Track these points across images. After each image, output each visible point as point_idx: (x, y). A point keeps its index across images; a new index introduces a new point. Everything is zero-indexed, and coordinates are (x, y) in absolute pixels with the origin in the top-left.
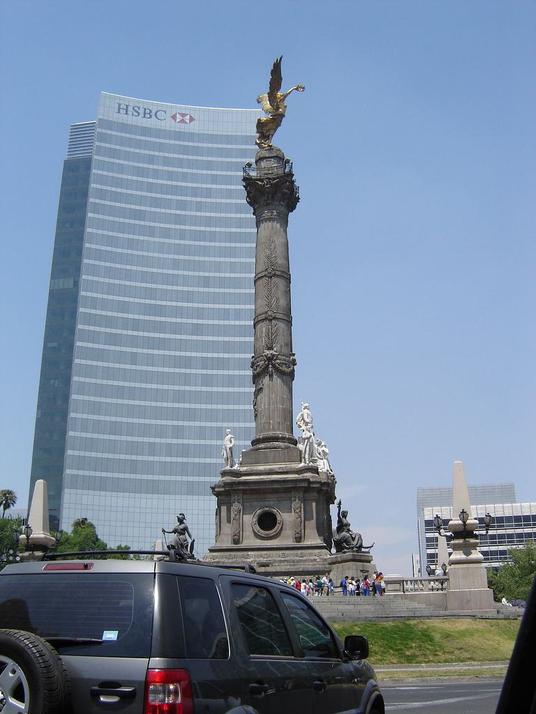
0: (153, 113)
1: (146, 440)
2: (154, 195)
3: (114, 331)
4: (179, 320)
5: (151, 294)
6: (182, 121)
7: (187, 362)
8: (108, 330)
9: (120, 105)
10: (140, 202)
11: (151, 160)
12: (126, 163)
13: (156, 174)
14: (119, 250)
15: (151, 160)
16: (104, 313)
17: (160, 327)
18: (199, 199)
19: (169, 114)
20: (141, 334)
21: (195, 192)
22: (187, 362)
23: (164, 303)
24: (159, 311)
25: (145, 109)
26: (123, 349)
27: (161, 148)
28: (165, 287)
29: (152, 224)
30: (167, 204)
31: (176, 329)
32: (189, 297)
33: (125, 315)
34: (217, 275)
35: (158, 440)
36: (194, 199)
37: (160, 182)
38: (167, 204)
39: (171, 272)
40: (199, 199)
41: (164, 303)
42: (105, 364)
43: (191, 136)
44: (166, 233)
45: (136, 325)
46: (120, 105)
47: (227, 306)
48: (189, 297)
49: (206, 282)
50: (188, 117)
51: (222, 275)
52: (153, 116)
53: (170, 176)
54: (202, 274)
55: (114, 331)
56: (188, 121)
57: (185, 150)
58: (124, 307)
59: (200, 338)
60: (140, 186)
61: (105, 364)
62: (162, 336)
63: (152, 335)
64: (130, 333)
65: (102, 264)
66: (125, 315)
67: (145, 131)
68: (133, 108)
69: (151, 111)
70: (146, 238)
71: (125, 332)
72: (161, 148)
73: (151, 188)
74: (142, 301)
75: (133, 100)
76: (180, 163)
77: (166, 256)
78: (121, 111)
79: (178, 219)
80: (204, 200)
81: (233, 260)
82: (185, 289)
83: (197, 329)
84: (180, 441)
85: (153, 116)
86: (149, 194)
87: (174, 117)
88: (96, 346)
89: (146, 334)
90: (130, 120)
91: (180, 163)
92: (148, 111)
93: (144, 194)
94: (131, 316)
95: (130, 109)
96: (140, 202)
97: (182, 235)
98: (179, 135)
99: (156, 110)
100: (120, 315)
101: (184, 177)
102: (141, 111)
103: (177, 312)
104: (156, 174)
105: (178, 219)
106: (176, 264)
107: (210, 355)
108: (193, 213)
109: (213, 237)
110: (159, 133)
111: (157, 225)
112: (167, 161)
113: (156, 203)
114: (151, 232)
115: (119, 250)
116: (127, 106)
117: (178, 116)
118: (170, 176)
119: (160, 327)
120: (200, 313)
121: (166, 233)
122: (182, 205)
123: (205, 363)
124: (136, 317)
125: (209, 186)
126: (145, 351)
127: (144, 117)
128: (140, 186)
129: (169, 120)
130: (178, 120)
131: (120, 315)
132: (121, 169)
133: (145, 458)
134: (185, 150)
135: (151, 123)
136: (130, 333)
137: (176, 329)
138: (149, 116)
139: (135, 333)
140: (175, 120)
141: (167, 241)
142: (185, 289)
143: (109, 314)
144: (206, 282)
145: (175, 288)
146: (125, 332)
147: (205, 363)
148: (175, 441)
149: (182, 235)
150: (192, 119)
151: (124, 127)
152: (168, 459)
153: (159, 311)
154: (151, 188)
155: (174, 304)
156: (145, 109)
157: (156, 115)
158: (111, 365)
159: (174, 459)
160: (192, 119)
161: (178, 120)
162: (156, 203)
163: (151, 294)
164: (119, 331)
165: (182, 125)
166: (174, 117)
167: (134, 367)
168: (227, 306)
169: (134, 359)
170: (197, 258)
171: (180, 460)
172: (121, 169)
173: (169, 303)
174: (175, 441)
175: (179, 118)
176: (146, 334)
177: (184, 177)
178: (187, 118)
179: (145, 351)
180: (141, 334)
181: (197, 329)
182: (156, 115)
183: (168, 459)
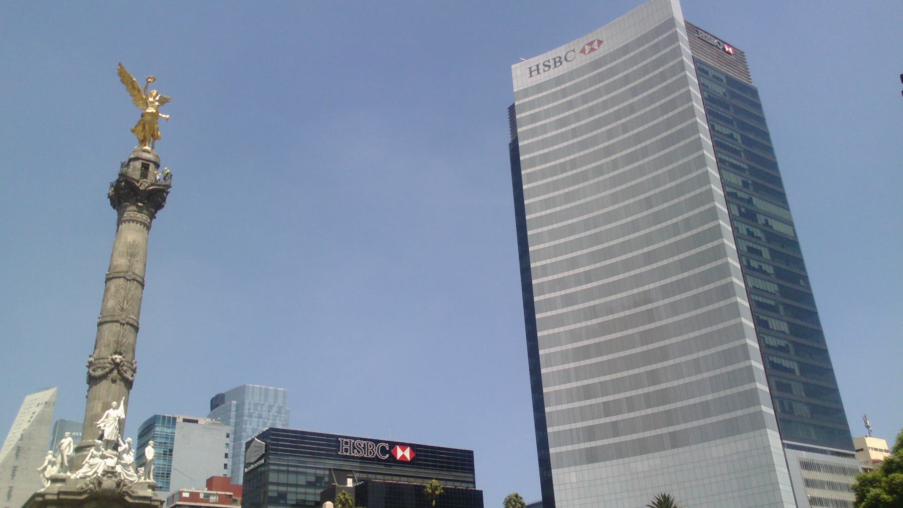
0: (563, 59)
3: (568, 291)
6: (592, 50)
19: (578, 51)
46: (530, 68)
50: (596, 43)
52: (564, 62)
55: (568, 291)
56: (596, 47)
68: (544, 65)
69: (560, 58)
75: (539, 59)
78: (533, 73)
85: (564, 62)
88: (554, 313)
92: (557, 60)
95: (541, 67)
99: (565, 53)
102: (552, 63)
116: (538, 66)
127: (555, 67)
133: (626, 416)
138: (559, 64)
140: (585, 53)
148: (652, 389)
150: (600, 42)
157: (566, 59)
165: (593, 54)
166: (583, 51)
171: (661, 408)
174: (652, 389)
182: (566, 59)
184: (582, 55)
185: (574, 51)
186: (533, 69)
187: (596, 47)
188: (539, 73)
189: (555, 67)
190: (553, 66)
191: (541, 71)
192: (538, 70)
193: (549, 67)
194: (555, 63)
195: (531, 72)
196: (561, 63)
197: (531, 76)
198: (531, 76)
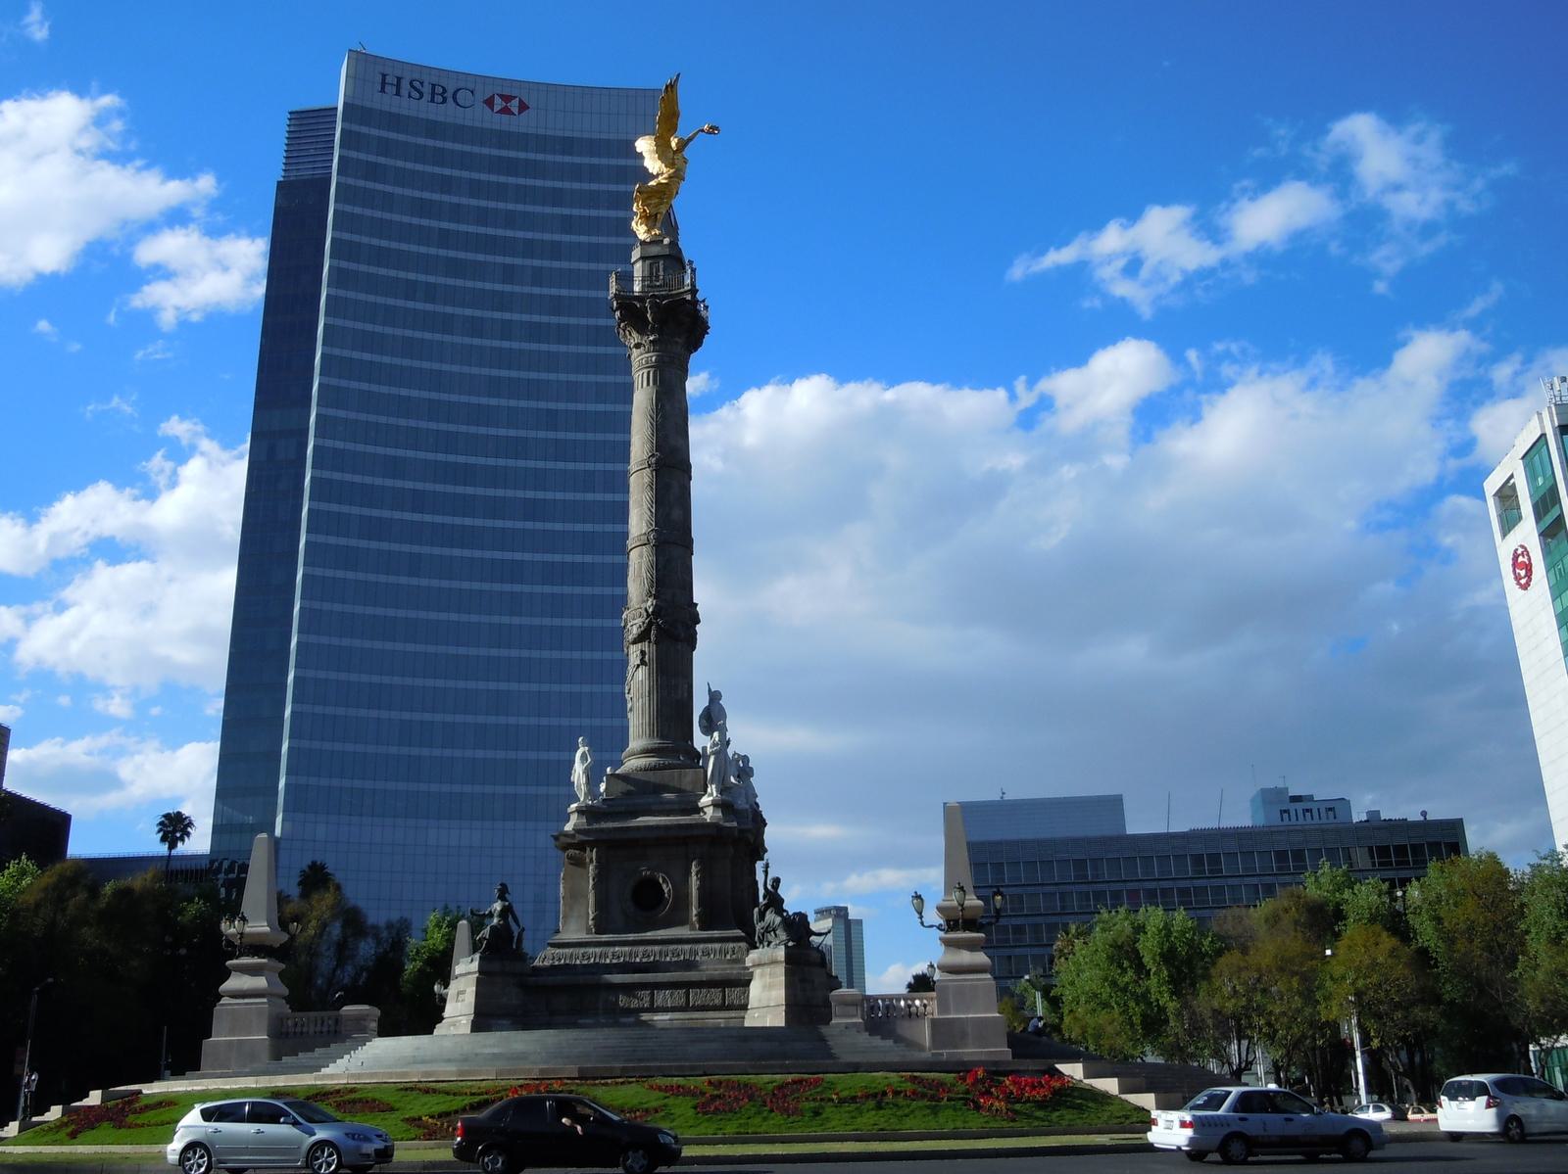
0: (449, 95)
1: (438, 717)
2: (452, 254)
3: (376, 513)
4: (500, 493)
5: (448, 442)
6: (506, 111)
7: (514, 572)
8: (366, 511)
9: (384, 76)
10: (426, 264)
11: (446, 185)
12: (398, 190)
13: (456, 213)
14: (386, 359)
15: (446, 185)
16: (357, 479)
17: (467, 506)
18: (537, 263)
19: (480, 97)
20: (428, 518)
21: (530, 249)
22: (514, 572)
23: (472, 460)
24: (465, 475)
25: (434, 86)
26: (395, 547)
27: (465, 161)
28: (473, 429)
29: (449, 310)
30: (479, 271)
31: (495, 508)
32: (518, 447)
33: (399, 483)
34: (571, 406)
35: (459, 718)
36: (528, 262)
37: (463, 228)
38: (479, 271)
39: (484, 401)
40: (537, 263)
41: (472, 460)
42: (361, 576)
43: (523, 140)
44: (476, 327)
45: (418, 501)
46: (384, 76)
47: (590, 466)
48: (518, 447)
49: (551, 420)
51: (581, 407)
53: (483, 217)
54: (542, 405)
55: (376, 513)
56: (515, 110)
57: (510, 167)
58: (395, 468)
59: (539, 525)
60: (423, 236)
61: (361, 576)
62: (468, 521)
63: (448, 520)
64: (407, 516)
65: (354, 385)
66: (399, 483)
67: (433, 129)
68: (411, 83)
70: (438, 337)
71: (397, 515)
72: (465, 161)
73: (445, 239)
74: (431, 456)
76: (499, 192)
77: (475, 370)
78: (388, 88)
79: (502, 302)
80: (546, 263)
81: (600, 378)
82: (512, 433)
83: (534, 510)
84: (502, 720)
85: (450, 100)
86: (442, 252)
87: (490, 102)
89: (438, 519)
90: (405, 106)
91: (499, 192)
93: (433, 251)
94: (409, 485)
95: (405, 85)
96: (426, 264)
97: (506, 330)
98: (504, 139)
100: (389, 482)
101: (510, 220)
102: (426, 90)
103: (495, 477)
104: (456, 213)
105: (502, 302)
106: (495, 387)
107: (557, 558)
108: (527, 289)
109: (563, 334)
110: (460, 132)
111: (458, 311)
112: (476, 189)
113: (455, 268)
114: (446, 324)
115: (386, 359)
116: (399, 79)
117: (498, 100)
118: (483, 217)
119: (467, 506)
120: (539, 479)
121: (476, 327)
122: (509, 274)
123: (551, 573)
124: (420, 486)
125: (557, 237)
126: (437, 551)
127: (432, 101)
128: (423, 236)
129: (480, 107)
130: (497, 108)
131: (389, 482)
132: (388, 201)
134: (510, 167)
135: (446, 113)
136: (407, 516)
137: (495, 508)
138: (440, 99)
139: (417, 517)
141: (476, 341)
142: (512, 433)
143: (368, 480)
144: (551, 420)
145: (492, 431)
146: (397, 515)
147: (551, 573)
149: (506, 330)
150: (523, 107)
151: (394, 121)
152: (480, 754)
153: (465, 475)
154: (445, 239)
155: (491, 461)
156: (434, 86)
158: (372, 577)
159: (490, 754)
160: (523, 107)
161: (497, 108)
162: (455, 268)
163: (448, 442)
164: (386, 514)
165: (505, 117)
166: (490, 102)
167: (414, 581)
168: (590, 466)
169: (415, 564)
170: (533, 375)
172: (388, 201)
173: (481, 460)
174: (492, 720)
175: (499, 103)
176: (438, 519)
177: (510, 220)
178: (514, 105)
179: (437, 551)
180: (428, 518)
181: (534, 510)
183: (480, 754)
184: (487, 110)
185: (472, 92)
186: (389, 79)
187: (515, 110)
188: (398, 93)
189: (432, 101)
190: (427, 97)
191: (404, 92)
192: (398, 86)
193: (421, 95)
194: (433, 93)
195: (384, 83)
196: (444, 101)
197: (383, 90)
198: (383, 90)
